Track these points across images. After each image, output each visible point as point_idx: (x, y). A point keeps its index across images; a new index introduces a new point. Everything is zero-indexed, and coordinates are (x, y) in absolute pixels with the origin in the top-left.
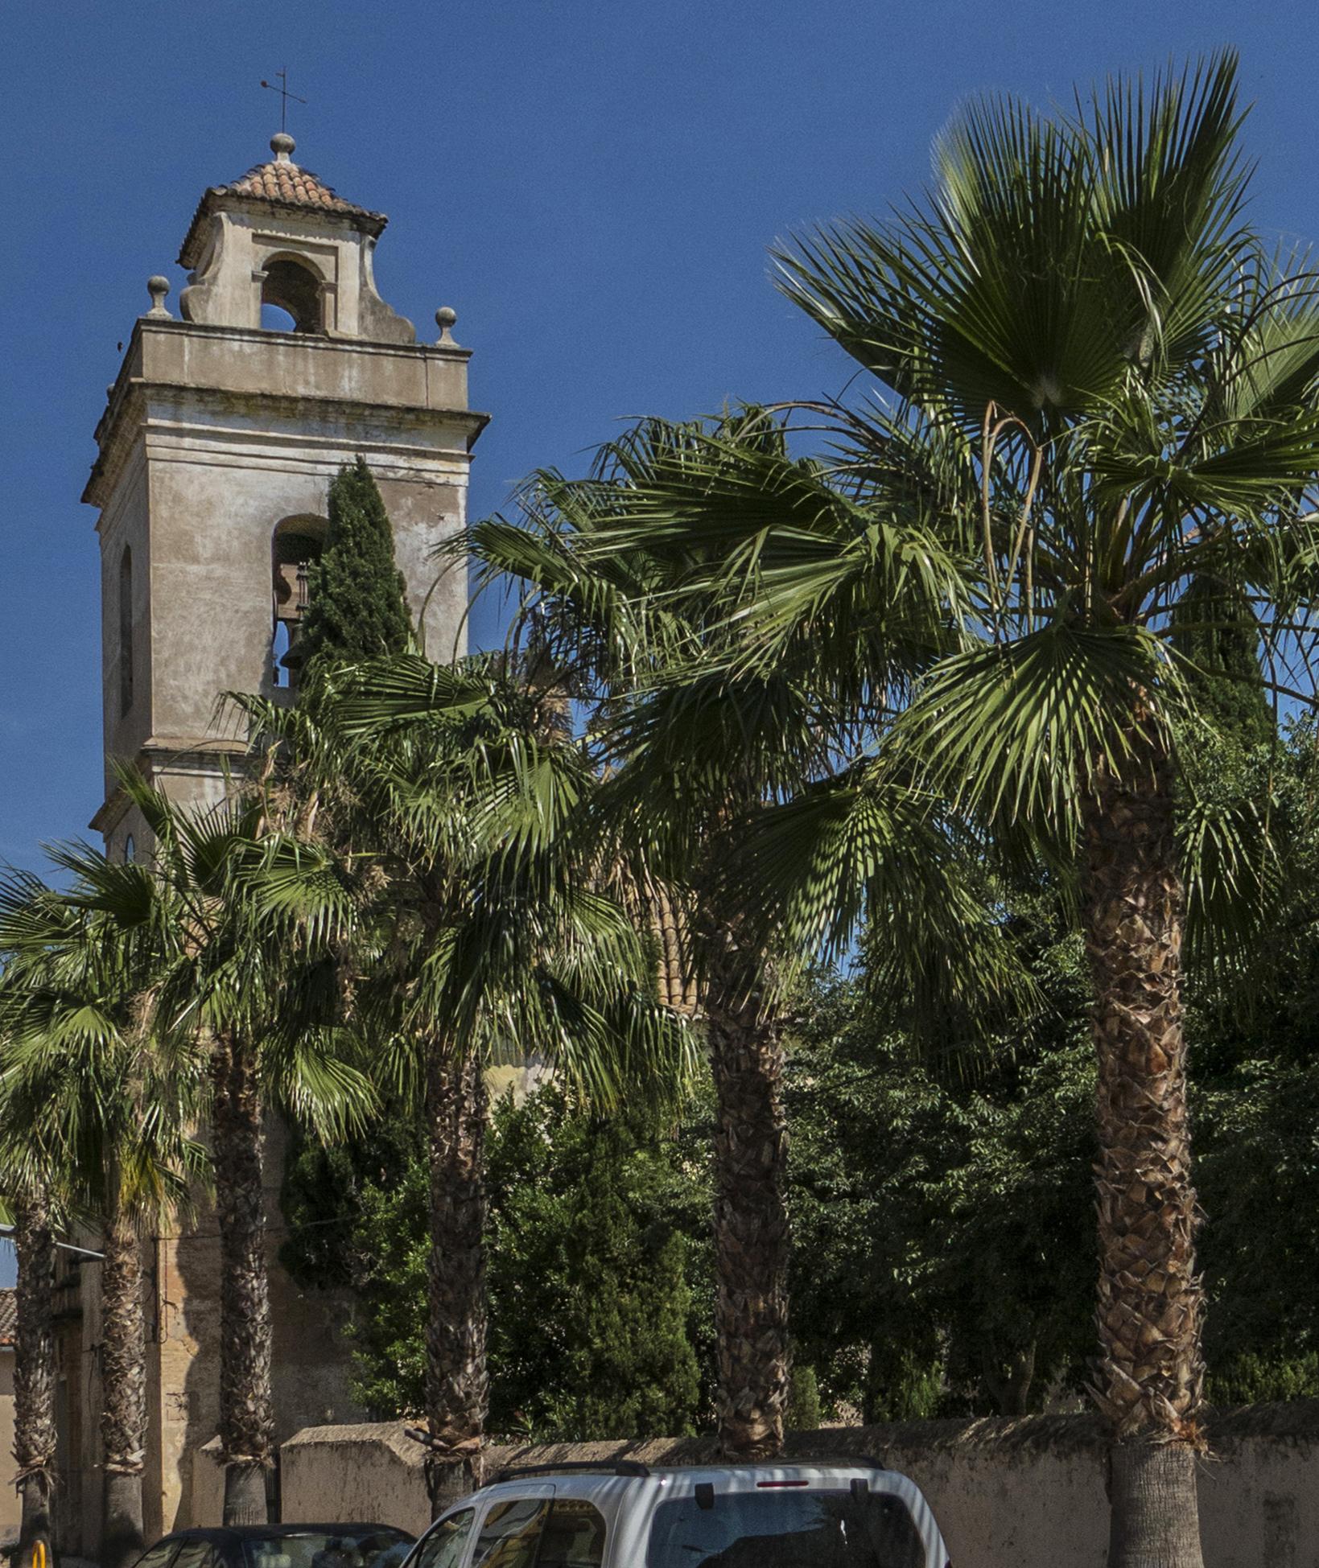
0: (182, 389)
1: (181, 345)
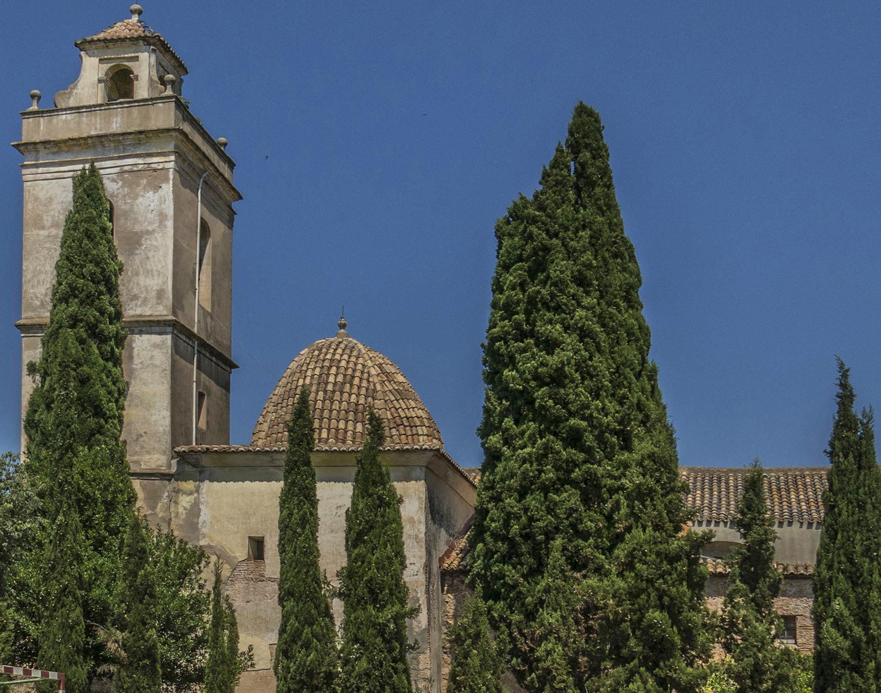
0: (35, 144)
1: (39, 122)
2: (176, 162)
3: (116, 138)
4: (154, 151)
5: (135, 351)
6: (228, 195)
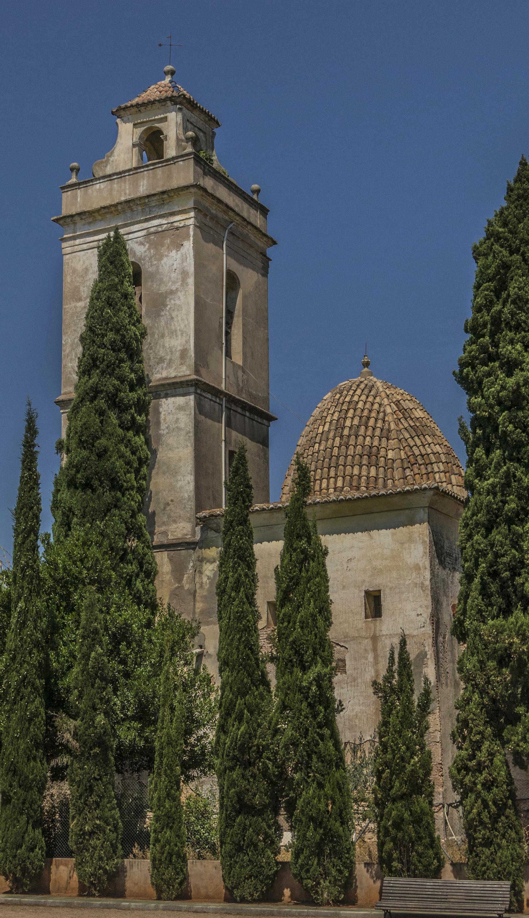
0: (72, 216)
1: (76, 194)
2: (195, 218)
3: (143, 201)
4: (176, 209)
5: (162, 416)
6: (260, 243)
